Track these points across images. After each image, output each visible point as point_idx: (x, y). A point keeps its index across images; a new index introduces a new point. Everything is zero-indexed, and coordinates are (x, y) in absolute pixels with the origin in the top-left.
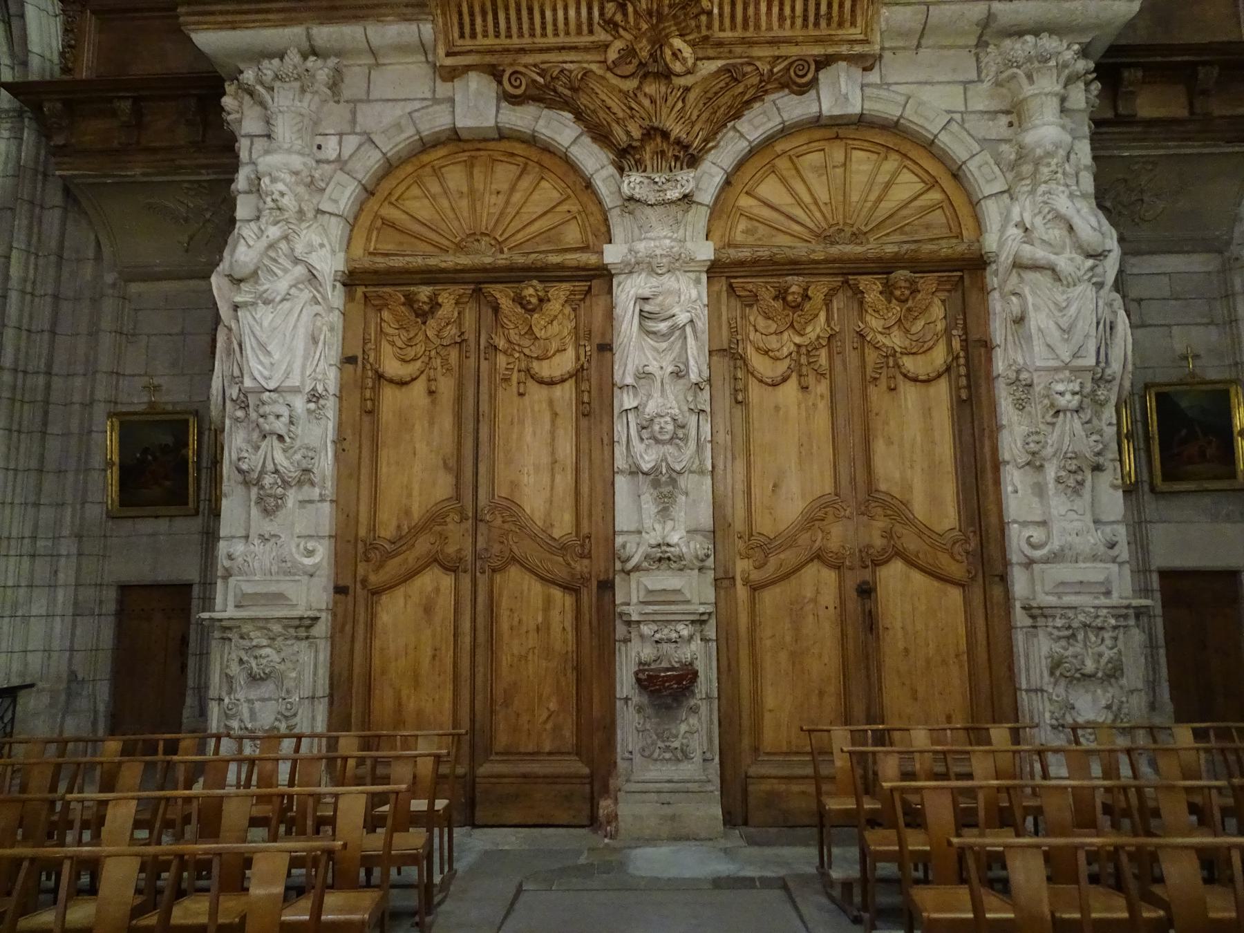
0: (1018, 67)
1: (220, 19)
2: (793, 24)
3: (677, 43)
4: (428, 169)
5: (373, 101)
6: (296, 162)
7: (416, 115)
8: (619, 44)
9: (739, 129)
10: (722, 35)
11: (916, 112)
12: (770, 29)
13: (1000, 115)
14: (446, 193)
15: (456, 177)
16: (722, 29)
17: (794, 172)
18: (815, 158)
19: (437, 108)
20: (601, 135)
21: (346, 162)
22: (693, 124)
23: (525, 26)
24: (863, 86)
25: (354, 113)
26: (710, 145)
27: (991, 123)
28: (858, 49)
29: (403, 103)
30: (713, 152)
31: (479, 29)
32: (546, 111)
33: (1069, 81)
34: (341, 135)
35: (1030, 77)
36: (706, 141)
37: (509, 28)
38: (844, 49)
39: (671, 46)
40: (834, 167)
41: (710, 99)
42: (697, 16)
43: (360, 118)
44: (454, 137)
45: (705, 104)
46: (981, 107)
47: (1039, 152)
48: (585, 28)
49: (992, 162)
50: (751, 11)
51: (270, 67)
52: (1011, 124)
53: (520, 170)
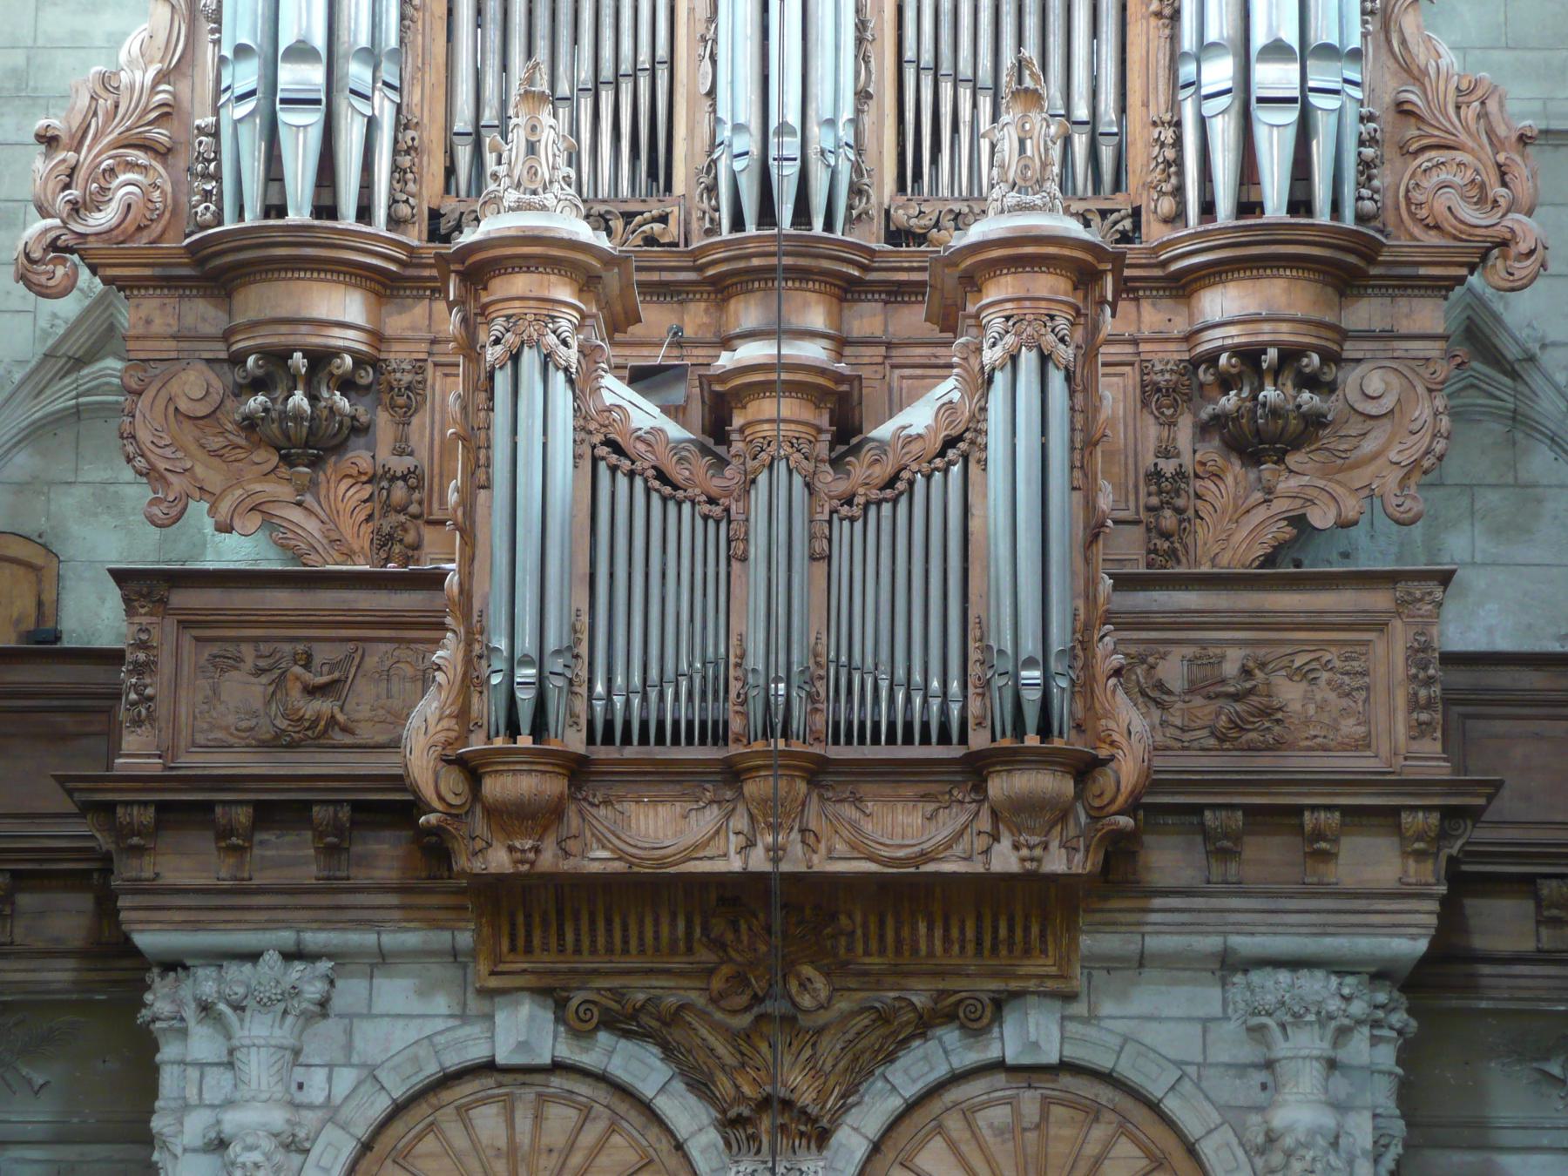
0: (1269, 1014)
1: (178, 916)
2: (962, 948)
3: (807, 970)
4: (450, 1110)
5: (377, 1016)
6: (278, 1118)
7: (441, 1039)
8: (725, 970)
9: (890, 1078)
10: (867, 960)
11: (1133, 1066)
12: (931, 954)
13: (1251, 1070)
14: (475, 1149)
15: (488, 1121)
16: (867, 953)
17: (968, 1135)
18: (1001, 1114)
19: (467, 1030)
20: (700, 1086)
21: (337, 1109)
22: (827, 1075)
23: (601, 941)
24: (1063, 1018)
25: (349, 1033)
26: (850, 1100)
27: (1238, 1081)
28: (1051, 985)
29: (419, 1021)
30: (853, 1110)
31: (536, 941)
32: (623, 1043)
33: (1343, 1033)
34: (331, 1067)
35: (1283, 1026)
36: (844, 1096)
37: (578, 941)
38: (1032, 985)
39: (798, 976)
40: (1024, 1130)
41: (851, 1041)
42: (834, 937)
43: (359, 1043)
44: (489, 1067)
45: (843, 1049)
46: (1225, 1058)
47: (1289, 1141)
48: (682, 945)
49: (1234, 1141)
50: (906, 933)
51: (239, 974)
52: (1264, 1087)
53: (582, 1117)
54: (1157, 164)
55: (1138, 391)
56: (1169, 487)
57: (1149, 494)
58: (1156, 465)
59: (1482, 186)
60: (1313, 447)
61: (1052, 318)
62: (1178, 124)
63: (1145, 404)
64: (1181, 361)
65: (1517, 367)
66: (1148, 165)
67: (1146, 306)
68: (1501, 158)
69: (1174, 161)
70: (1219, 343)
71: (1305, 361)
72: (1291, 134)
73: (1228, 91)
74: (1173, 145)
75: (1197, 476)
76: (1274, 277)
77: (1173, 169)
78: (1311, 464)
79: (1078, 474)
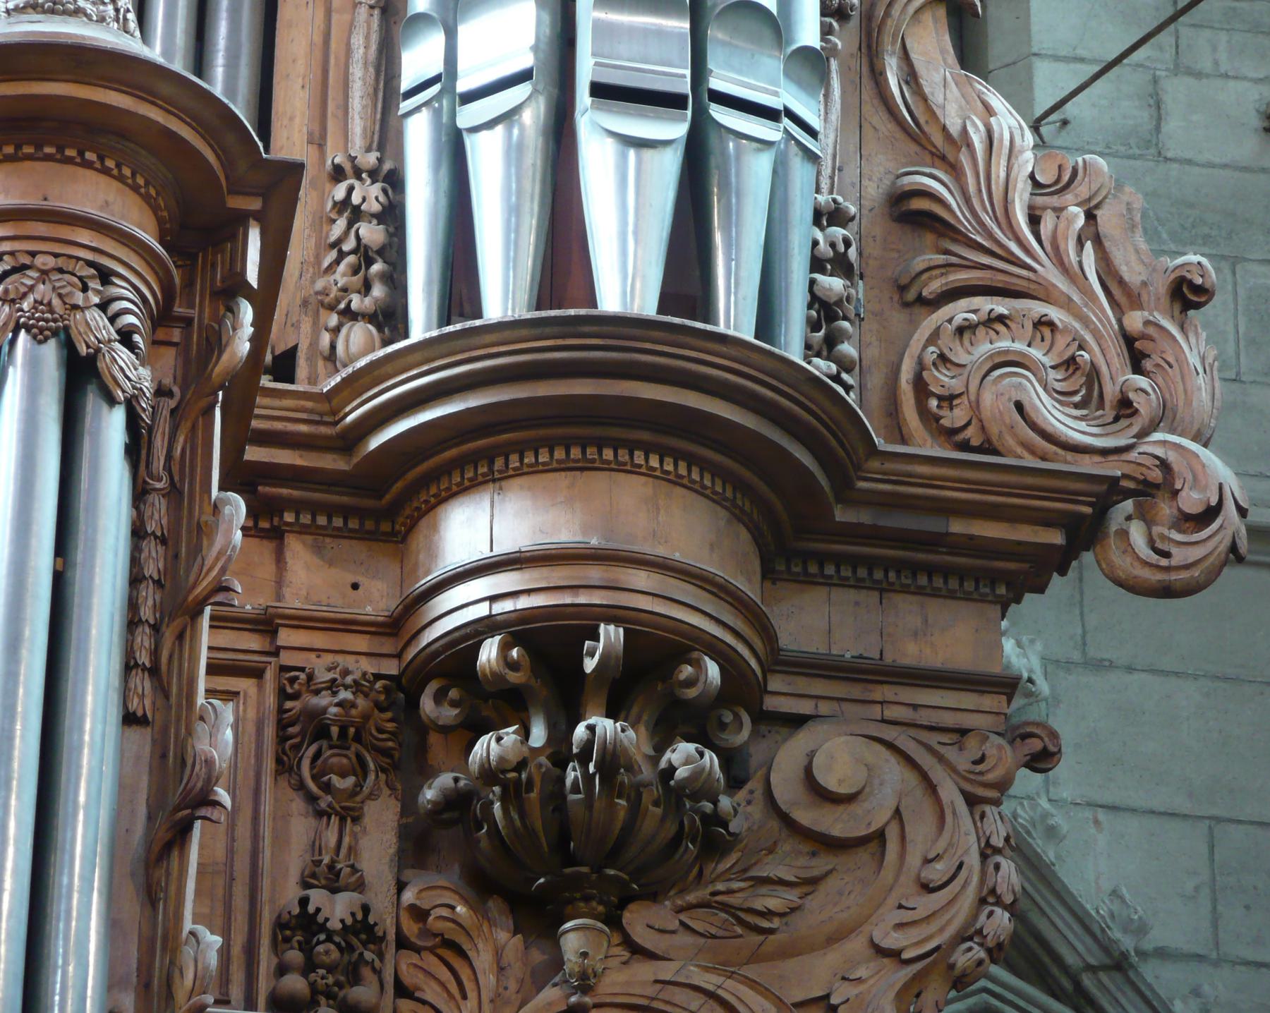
54: (342, 255)
55: (270, 732)
56: (335, 954)
57: (282, 970)
58: (304, 902)
59: (1093, 375)
60: (691, 898)
61: (105, 276)
62: (394, 181)
63: (284, 766)
64: (378, 677)
65: (1087, 981)
66: (318, 259)
67: (297, 551)
68: (1135, 321)
69: (381, 252)
70: (482, 610)
71: (687, 671)
72: (668, 165)
73: (523, 77)
74: (380, 218)
75: (402, 943)
76: (620, 468)
77: (377, 267)
78: (685, 939)
79: (142, 683)
